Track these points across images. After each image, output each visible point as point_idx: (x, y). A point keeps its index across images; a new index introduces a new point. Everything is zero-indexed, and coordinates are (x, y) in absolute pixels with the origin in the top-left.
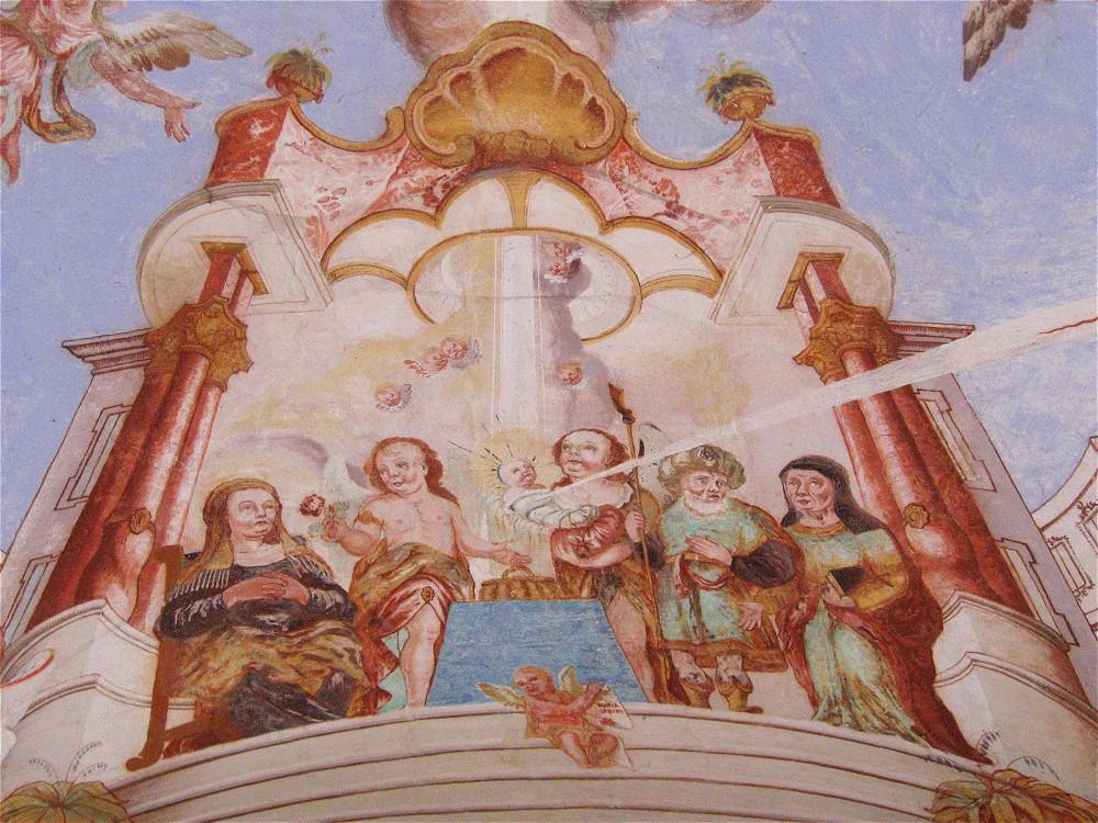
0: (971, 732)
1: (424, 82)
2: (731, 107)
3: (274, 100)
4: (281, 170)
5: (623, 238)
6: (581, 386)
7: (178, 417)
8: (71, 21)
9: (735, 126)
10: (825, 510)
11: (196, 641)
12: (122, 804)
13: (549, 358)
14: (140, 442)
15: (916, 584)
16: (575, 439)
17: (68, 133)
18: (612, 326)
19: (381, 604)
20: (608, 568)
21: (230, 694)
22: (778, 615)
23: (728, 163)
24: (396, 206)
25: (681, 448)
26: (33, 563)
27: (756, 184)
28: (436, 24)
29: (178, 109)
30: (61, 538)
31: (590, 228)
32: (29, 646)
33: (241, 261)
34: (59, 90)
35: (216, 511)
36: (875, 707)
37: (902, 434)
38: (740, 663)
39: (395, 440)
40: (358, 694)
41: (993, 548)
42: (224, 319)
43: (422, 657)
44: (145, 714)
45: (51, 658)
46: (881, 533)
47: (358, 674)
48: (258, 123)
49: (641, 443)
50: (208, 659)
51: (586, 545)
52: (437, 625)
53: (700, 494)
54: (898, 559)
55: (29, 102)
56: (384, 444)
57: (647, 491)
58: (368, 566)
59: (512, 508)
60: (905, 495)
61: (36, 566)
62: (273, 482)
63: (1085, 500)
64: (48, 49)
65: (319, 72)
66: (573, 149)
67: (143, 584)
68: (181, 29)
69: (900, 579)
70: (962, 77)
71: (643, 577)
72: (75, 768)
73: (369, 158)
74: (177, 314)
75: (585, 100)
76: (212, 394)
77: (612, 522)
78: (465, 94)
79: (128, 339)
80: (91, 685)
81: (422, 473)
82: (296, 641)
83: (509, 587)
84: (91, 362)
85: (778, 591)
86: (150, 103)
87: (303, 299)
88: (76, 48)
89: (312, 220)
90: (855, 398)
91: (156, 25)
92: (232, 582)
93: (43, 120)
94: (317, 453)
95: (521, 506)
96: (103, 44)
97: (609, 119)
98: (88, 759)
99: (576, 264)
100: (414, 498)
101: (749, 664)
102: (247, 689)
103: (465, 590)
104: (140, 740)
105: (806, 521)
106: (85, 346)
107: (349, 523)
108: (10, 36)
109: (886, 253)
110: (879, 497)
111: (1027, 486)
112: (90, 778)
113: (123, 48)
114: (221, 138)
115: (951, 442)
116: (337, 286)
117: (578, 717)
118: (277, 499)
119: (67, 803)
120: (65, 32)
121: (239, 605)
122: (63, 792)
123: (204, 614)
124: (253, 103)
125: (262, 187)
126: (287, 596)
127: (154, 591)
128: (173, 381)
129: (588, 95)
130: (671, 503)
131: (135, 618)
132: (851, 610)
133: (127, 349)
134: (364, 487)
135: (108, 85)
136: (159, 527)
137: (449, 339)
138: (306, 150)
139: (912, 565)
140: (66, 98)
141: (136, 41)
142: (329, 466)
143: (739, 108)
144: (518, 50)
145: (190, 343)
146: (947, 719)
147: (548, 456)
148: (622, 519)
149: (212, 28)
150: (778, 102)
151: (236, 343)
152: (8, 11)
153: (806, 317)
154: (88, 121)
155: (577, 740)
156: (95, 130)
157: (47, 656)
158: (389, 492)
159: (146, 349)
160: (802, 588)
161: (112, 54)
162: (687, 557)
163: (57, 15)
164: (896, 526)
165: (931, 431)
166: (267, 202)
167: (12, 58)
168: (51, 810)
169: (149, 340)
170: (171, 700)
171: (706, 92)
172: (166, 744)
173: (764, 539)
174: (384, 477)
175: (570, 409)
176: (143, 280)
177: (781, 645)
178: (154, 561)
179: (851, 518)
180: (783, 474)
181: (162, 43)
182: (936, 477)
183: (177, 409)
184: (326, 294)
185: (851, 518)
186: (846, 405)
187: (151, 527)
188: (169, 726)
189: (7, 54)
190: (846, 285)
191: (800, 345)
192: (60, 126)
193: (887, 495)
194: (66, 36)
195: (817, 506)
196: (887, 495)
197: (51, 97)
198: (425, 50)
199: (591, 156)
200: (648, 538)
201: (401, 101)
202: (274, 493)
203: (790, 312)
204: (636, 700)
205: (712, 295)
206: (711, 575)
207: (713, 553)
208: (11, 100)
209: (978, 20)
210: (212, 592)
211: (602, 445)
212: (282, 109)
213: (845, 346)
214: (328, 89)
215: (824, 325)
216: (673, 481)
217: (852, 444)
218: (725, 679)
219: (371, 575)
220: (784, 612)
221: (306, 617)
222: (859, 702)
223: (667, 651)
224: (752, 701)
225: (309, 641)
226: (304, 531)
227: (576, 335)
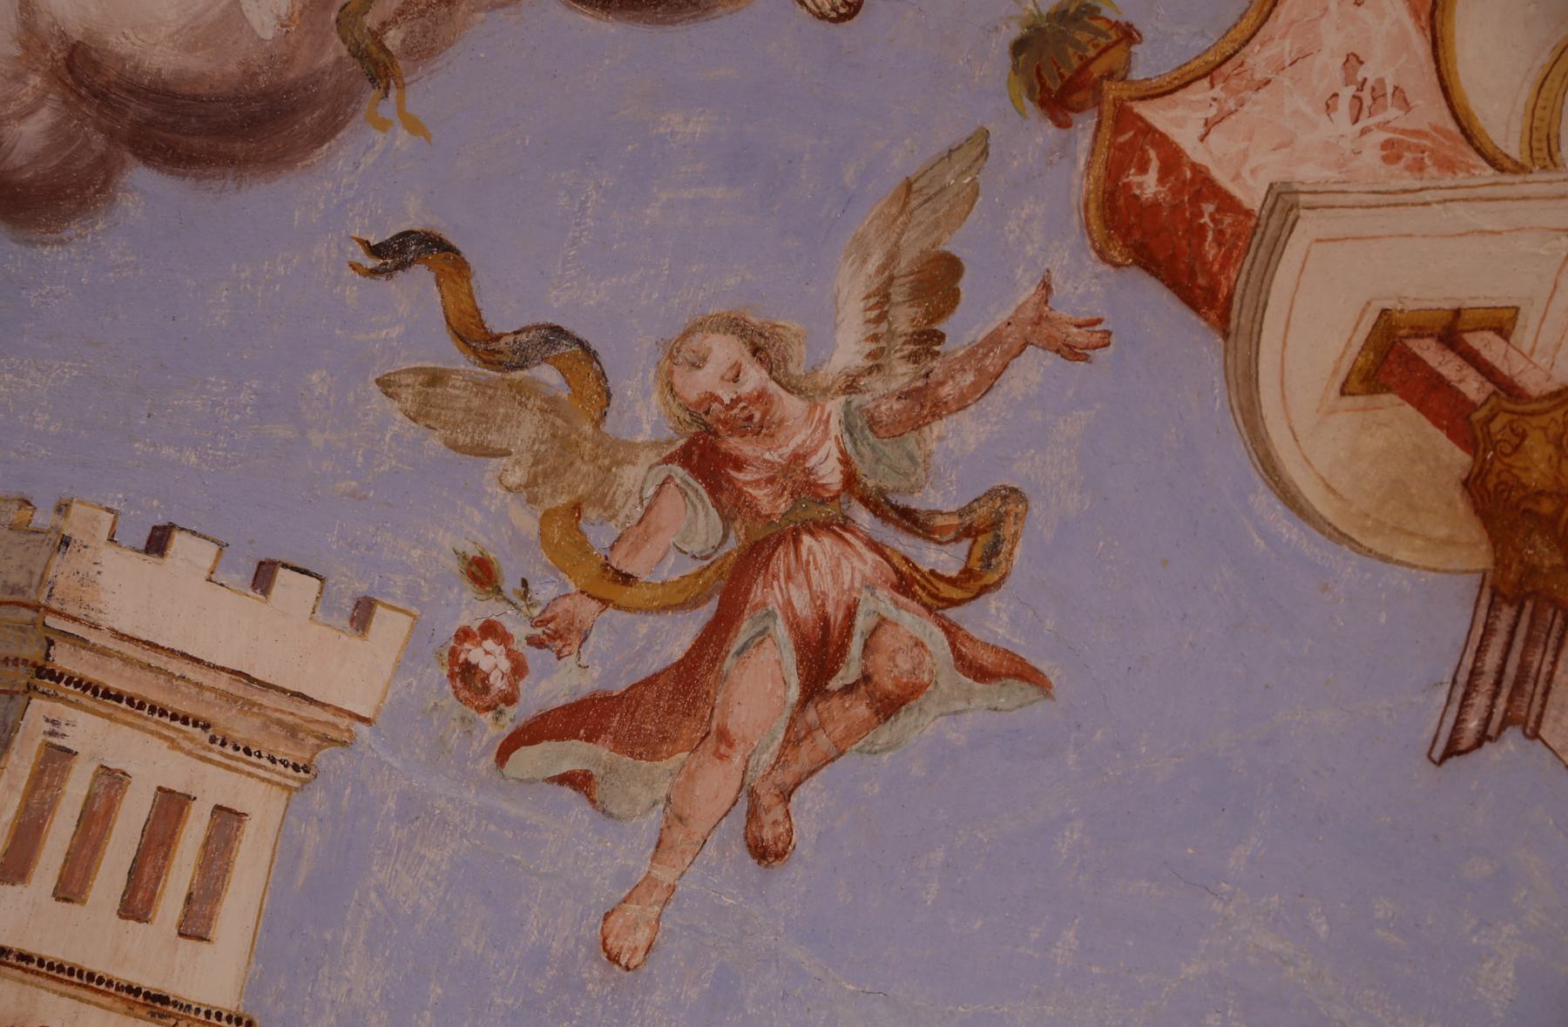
3: (1099, 124)
8: (789, 438)
17: (997, 543)
29: (1040, 320)
33: (1419, 332)
34: (910, 521)
42: (1535, 421)
48: (1133, 177)
55: (906, 582)
64: (824, 502)
68: (889, 245)
74: (1477, 512)
79: (1488, 631)
86: (1005, 366)
88: (843, 452)
89: (1392, 153)
93: (954, 573)
96: (856, 400)
106: (1459, 721)
108: (769, 558)
113: (879, 367)
114: (1136, 262)
120: (805, 457)
124: (1089, 166)
135: (938, 427)
138: (1231, 104)
141: (875, 338)
149: (908, 186)
152: (725, 537)
154: (992, 494)
156: (1014, 491)
159: (1529, 605)
161: (882, 393)
163: (767, 456)
166: (1308, 228)
167: (814, 574)
176: (1368, 542)
181: (898, 293)
189: (801, 577)
194: (812, 462)
197: (919, 541)
208: (889, 610)
212: (1124, 117)
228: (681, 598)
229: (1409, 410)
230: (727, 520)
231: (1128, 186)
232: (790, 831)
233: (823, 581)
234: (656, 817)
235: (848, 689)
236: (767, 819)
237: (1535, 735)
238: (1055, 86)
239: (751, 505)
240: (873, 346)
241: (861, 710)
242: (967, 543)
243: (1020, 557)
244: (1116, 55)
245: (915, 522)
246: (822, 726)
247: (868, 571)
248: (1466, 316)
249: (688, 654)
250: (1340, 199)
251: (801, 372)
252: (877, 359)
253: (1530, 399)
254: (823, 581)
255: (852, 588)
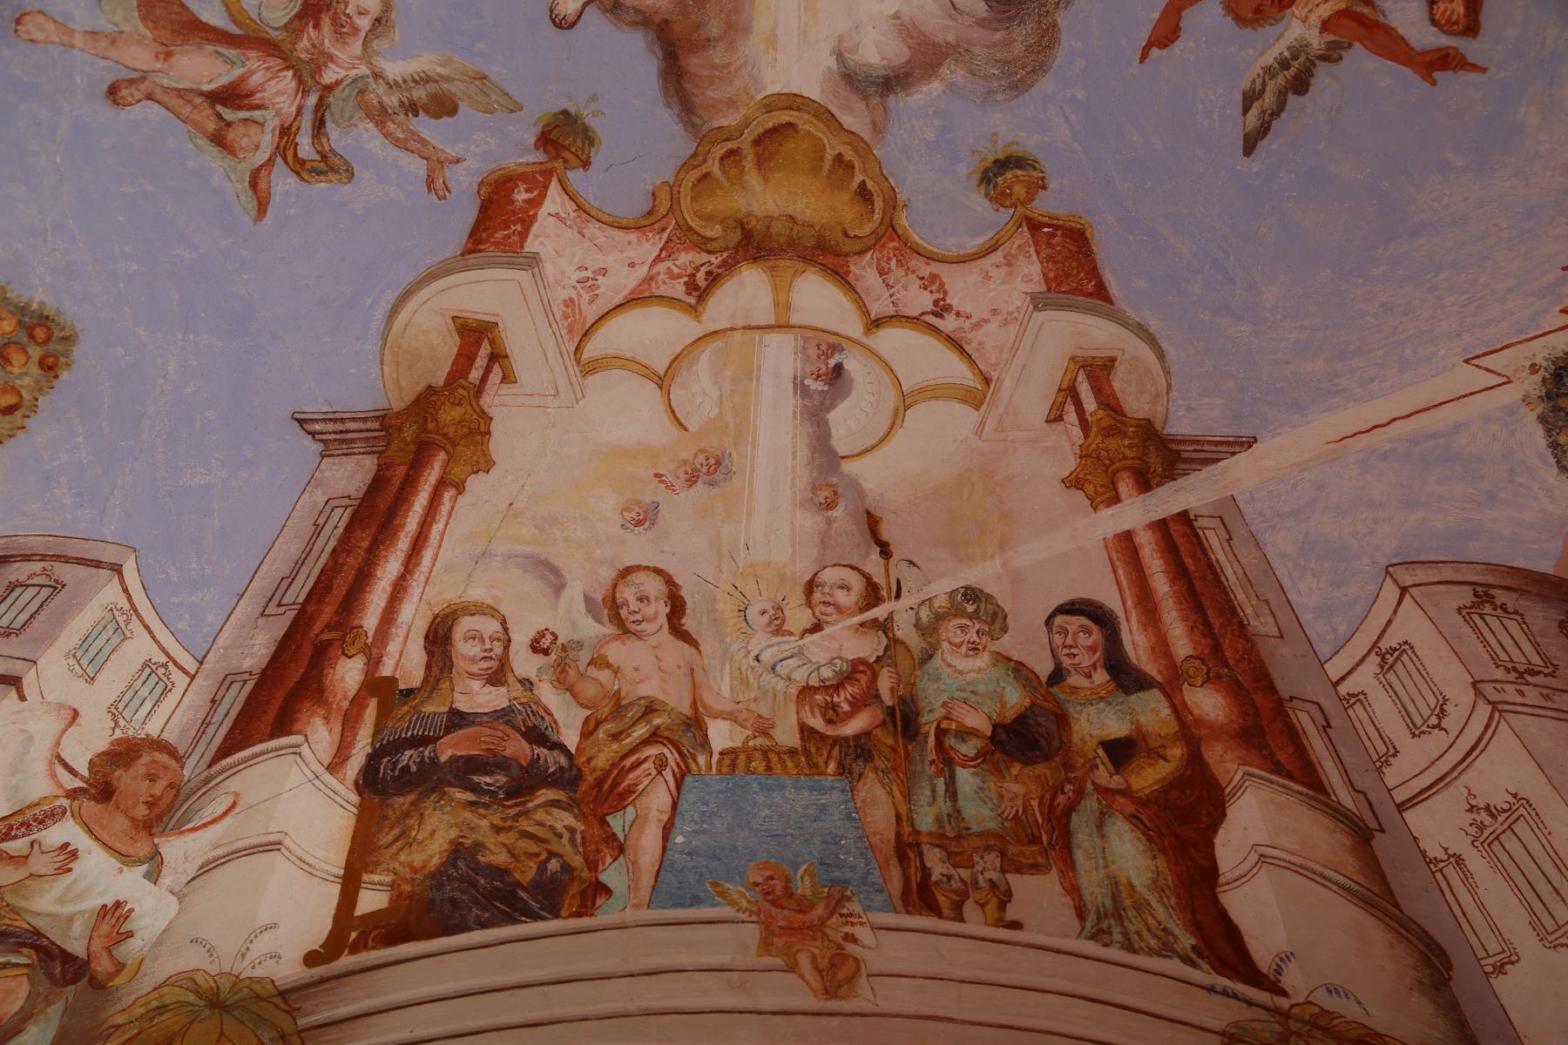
0: (1262, 950)
1: (694, 155)
2: (1003, 193)
4: (541, 243)
5: (891, 340)
6: (838, 512)
7: (409, 519)
9: (1005, 214)
10: (1094, 666)
11: (401, 802)
12: (292, 1013)
13: (804, 479)
14: (365, 544)
15: (1195, 758)
16: (829, 576)
18: (873, 442)
19: (609, 772)
20: (857, 737)
21: (432, 875)
22: (1041, 798)
23: (998, 256)
24: (657, 293)
25: (941, 588)
26: (230, 679)
27: (1027, 279)
28: (710, 93)
29: (440, 162)
30: (264, 651)
31: (854, 327)
32: (211, 785)
34: (319, 125)
35: (439, 638)
36: (1150, 921)
37: (1179, 571)
38: (998, 862)
39: (638, 568)
40: (575, 888)
41: (1280, 709)
42: (468, 407)
43: (648, 843)
44: (332, 893)
45: (234, 804)
46: (1155, 693)
47: (577, 861)
48: (522, 187)
49: (898, 582)
50: (411, 828)
51: (834, 707)
52: (668, 802)
53: (959, 646)
54: (1174, 727)
55: (287, 132)
56: (626, 572)
57: (903, 643)
58: (598, 724)
59: (757, 658)
60: (1182, 645)
61: (232, 683)
62: (503, 609)
63: (1384, 645)
64: (313, 77)
65: (588, 137)
66: (841, 237)
67: (350, 722)
68: (452, 75)
69: (1177, 752)
70: (1241, 152)
71: (894, 750)
72: (243, 956)
73: (633, 236)
75: (855, 184)
76: (447, 496)
77: (864, 679)
78: (734, 172)
79: (364, 420)
80: (274, 846)
81: (664, 610)
82: (513, 812)
83: (749, 760)
84: (321, 441)
85: (1042, 769)
86: (412, 152)
87: (552, 392)
88: (342, 80)
89: (569, 303)
90: (1126, 528)
91: (427, 67)
92: (448, 730)
93: (300, 155)
94: (554, 578)
95: (767, 657)
96: (371, 80)
97: (879, 204)
98: (261, 946)
99: (839, 368)
100: (653, 640)
101: (1011, 865)
102: (452, 871)
103: (701, 760)
104: (326, 925)
105: (1075, 680)
107: (582, 666)
108: (274, 56)
109: (1161, 355)
110: (1153, 649)
111: (1317, 629)
112: (259, 972)
113: (391, 87)
115: (1232, 578)
116: (591, 379)
117: (816, 930)
118: (506, 630)
119: (227, 1003)
120: (333, 61)
121: (453, 759)
122: (225, 985)
123: (414, 768)
124: (521, 164)
125: (521, 260)
126: (507, 753)
127: (361, 732)
128: (407, 474)
129: (859, 177)
130: (928, 656)
131: (334, 767)
132: (1122, 793)
133: (361, 431)
134: (601, 623)
135: (371, 126)
136: (375, 652)
137: (701, 451)
138: (569, 223)
139: (1190, 731)
140: (327, 135)
141: (405, 81)
142: (566, 594)
143: (1011, 195)
144: (791, 126)
145: (430, 432)
146: (1233, 934)
147: (798, 597)
148: (875, 676)
149: (484, 78)
150: (1052, 186)
151: (478, 438)
152: (276, 29)
153: (1077, 432)
154: (347, 163)
155: (814, 959)
156: (353, 174)
157: (229, 800)
158: (627, 631)
159: (383, 433)
160: (1068, 766)
162: (944, 725)
163: (326, 41)
164: (1171, 689)
165: (1210, 565)
166: (523, 276)
167: (273, 82)
168: (207, 1011)
169: (387, 423)
170: (365, 877)
171: (977, 177)
172: (353, 935)
173: (1027, 702)
174: (624, 612)
175: (825, 541)
177: (1045, 838)
178: (364, 694)
179: (1125, 677)
180: (1049, 622)
182: (1216, 622)
183: (409, 510)
184: (577, 388)
185: (1125, 677)
186: (1117, 536)
187: (366, 650)
188: (359, 912)
189: (270, 75)
190: (1119, 394)
191: (1069, 465)
192: (315, 165)
193: (1162, 647)
195: (1086, 660)
196: (1162, 647)
197: (310, 133)
198: (697, 121)
199: (858, 246)
200: (902, 699)
201: (669, 176)
202: (504, 623)
203: (1059, 426)
204: (882, 909)
205: (977, 408)
206: (969, 748)
207: (974, 720)
209: (1258, 87)
210: (425, 741)
211: (857, 583)
212: (548, 174)
213: (1117, 465)
214: (599, 157)
215: (1096, 441)
216: (929, 630)
217: (1124, 583)
218: (982, 882)
219: (601, 734)
220: (1048, 796)
221: (525, 783)
222: (1131, 913)
223: (918, 845)
224: (1011, 913)
225: (526, 813)
226: (532, 674)
227: (834, 452)
228: (234, 13)
229: (455, 350)
230: (285, 27)
231: (517, 186)
232: (130, 104)
233: (272, 87)
234: (109, 28)
235: (219, 116)
236: (132, 90)
237: (323, 457)
238: (553, 136)
239: (298, 39)
240: (401, 82)
241: (211, 126)
242: (318, 158)
243: (320, 187)
244: (574, 161)
245: (319, 128)
246: (195, 107)
247: (285, 110)
248: (506, 361)
249: (206, 24)
250: (541, 287)
251: (375, 48)
252: (392, 86)
253: (477, 402)
254: (272, 87)
255: (274, 104)
